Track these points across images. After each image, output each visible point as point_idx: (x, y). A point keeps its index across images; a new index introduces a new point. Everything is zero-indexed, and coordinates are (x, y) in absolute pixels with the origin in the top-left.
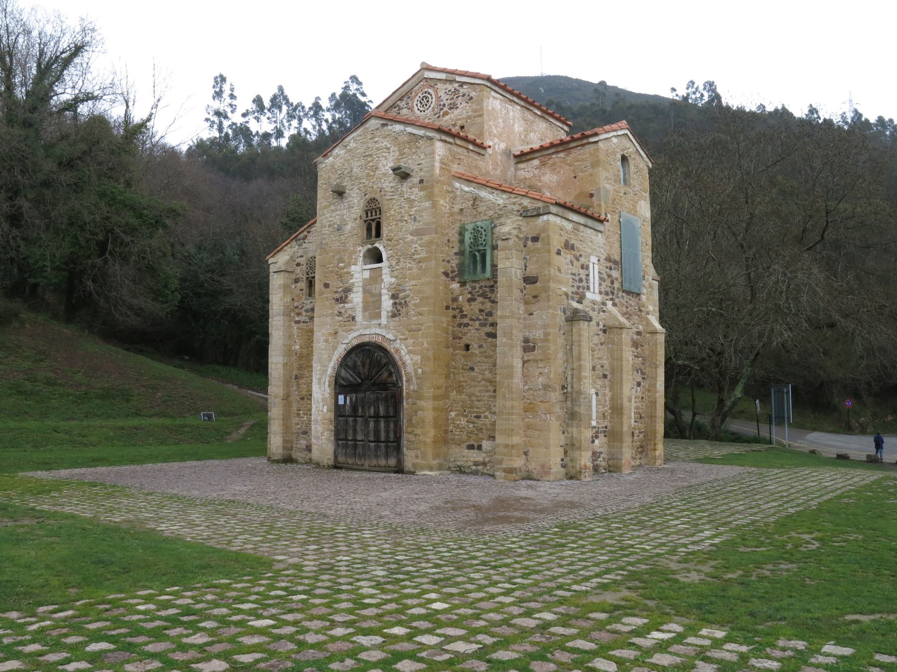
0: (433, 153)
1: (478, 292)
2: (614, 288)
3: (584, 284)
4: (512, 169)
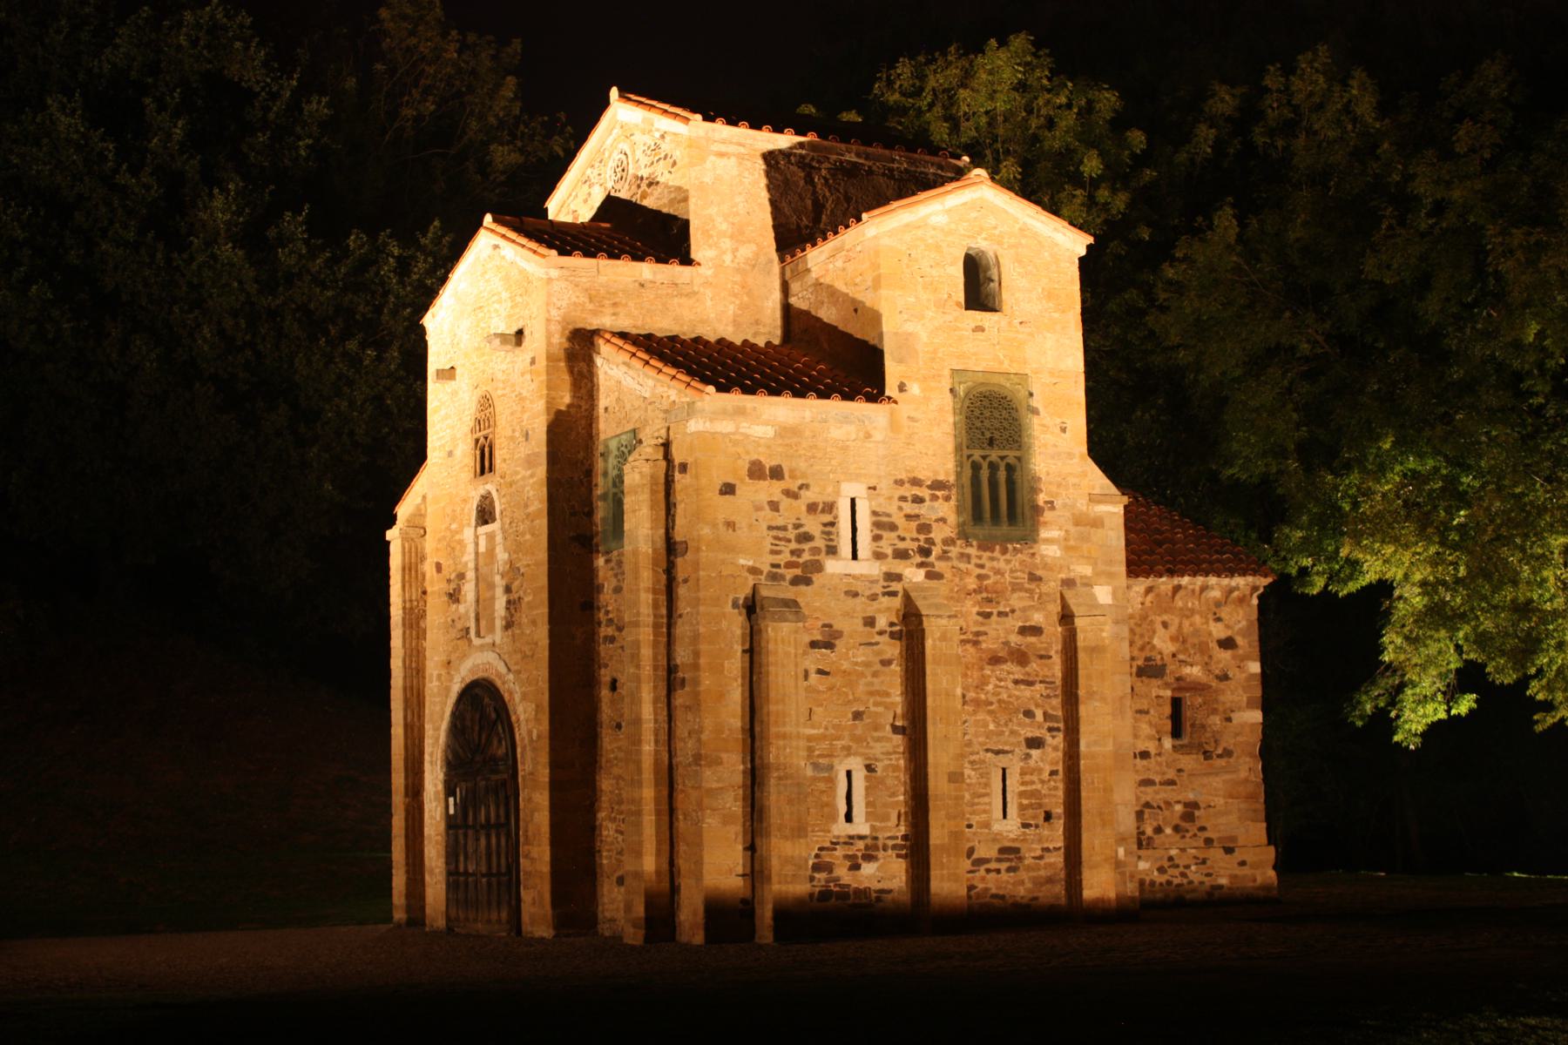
2: (931, 542)
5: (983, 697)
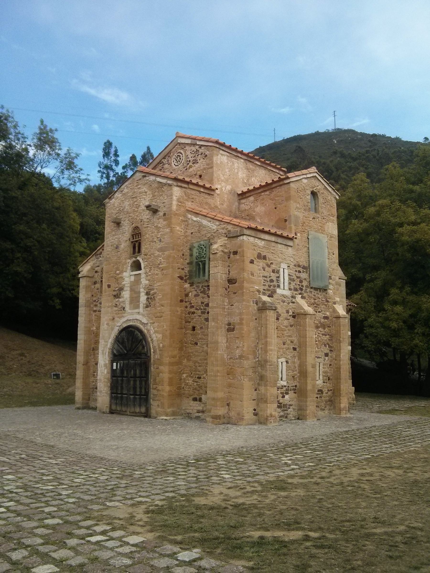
0: (172, 195)
1: (201, 290)
2: (302, 286)
3: (275, 283)
4: (237, 204)
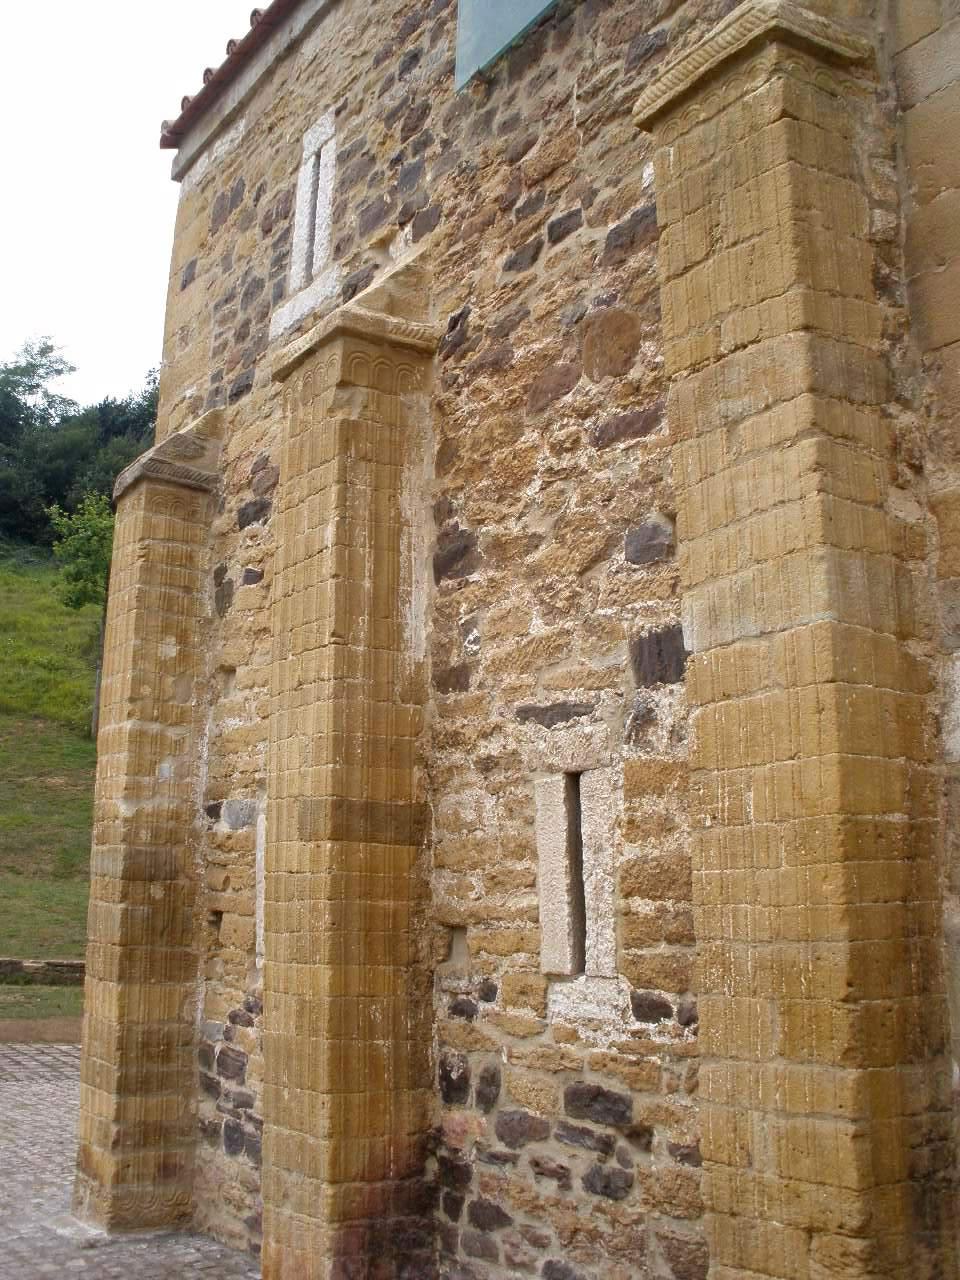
5: (515, 528)
